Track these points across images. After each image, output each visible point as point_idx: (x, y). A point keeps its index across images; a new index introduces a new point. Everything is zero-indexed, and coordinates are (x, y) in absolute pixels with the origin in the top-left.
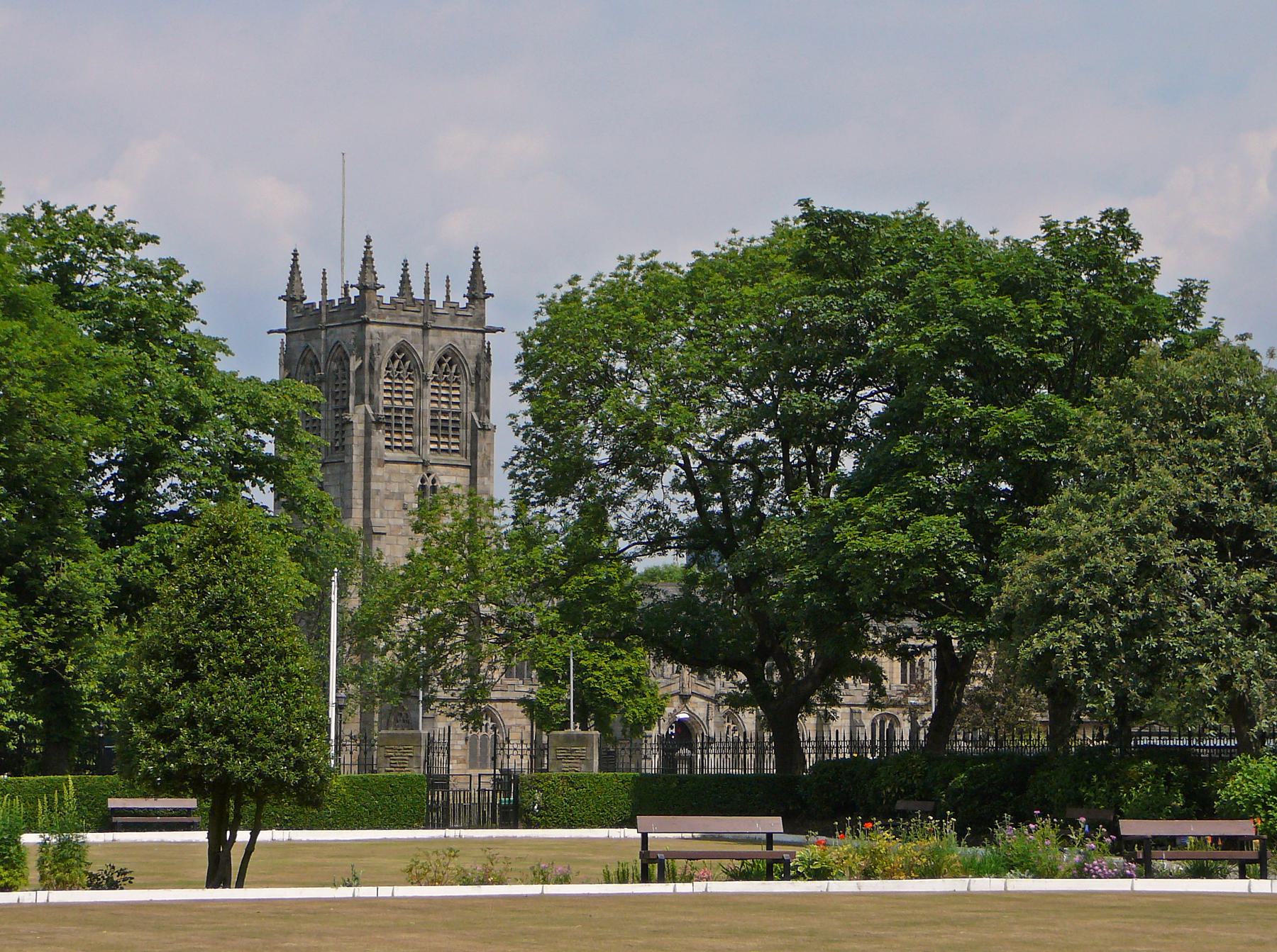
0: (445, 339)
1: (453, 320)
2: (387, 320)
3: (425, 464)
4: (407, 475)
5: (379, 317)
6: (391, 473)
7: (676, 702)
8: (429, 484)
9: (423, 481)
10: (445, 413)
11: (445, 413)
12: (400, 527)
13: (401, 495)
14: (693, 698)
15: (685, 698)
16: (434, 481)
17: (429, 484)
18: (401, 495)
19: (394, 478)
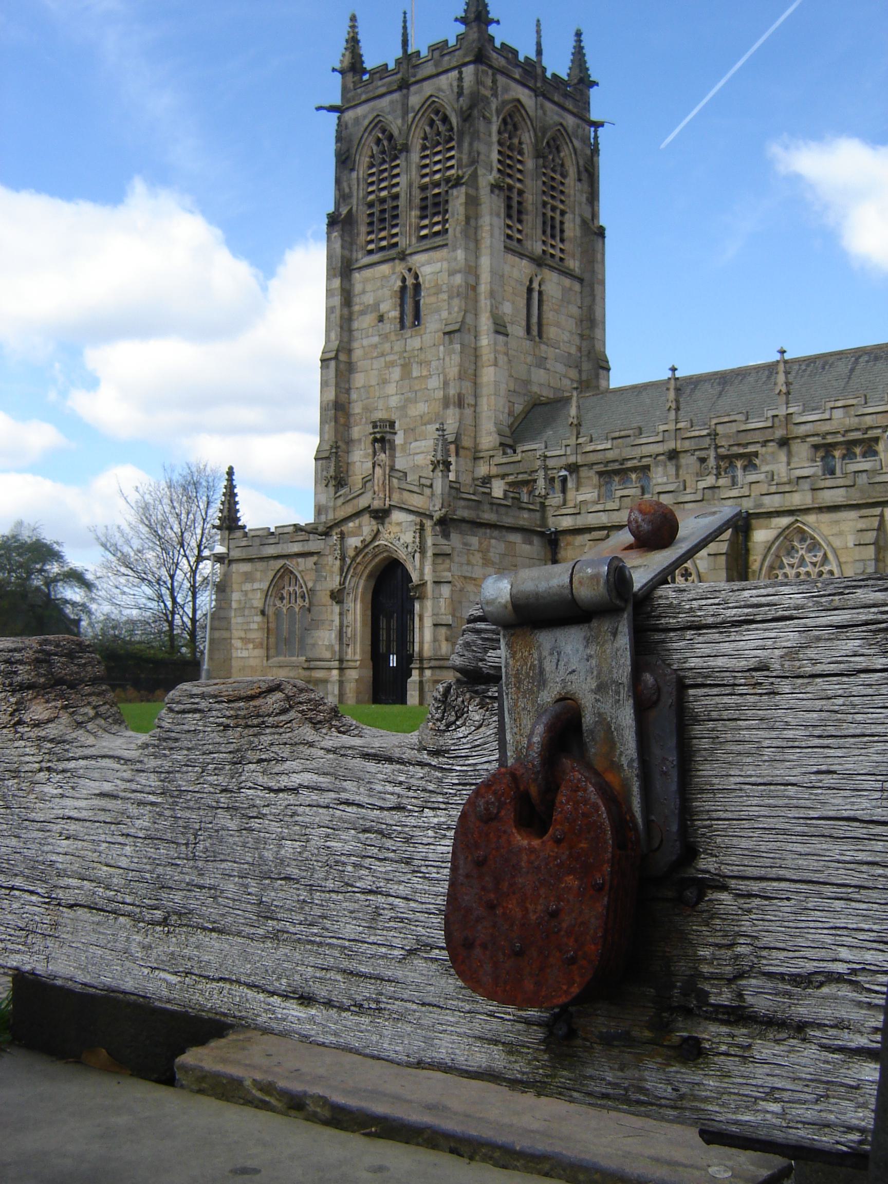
0: (428, 88)
1: (436, 65)
2: (364, 97)
3: (403, 257)
4: (384, 277)
5: (354, 100)
6: (365, 281)
7: (367, 526)
8: (410, 281)
9: (404, 280)
10: (437, 185)
11: (437, 185)
12: (375, 346)
13: (376, 305)
14: (397, 516)
15: (381, 515)
16: (416, 277)
17: (410, 281)
18: (376, 305)
19: (369, 287)
